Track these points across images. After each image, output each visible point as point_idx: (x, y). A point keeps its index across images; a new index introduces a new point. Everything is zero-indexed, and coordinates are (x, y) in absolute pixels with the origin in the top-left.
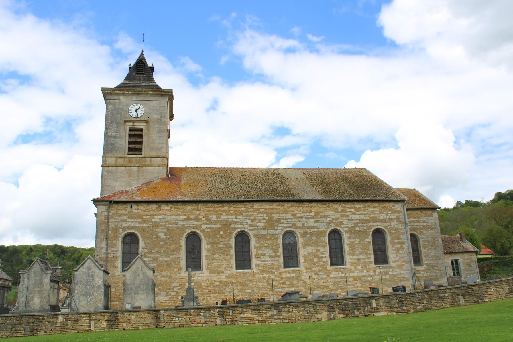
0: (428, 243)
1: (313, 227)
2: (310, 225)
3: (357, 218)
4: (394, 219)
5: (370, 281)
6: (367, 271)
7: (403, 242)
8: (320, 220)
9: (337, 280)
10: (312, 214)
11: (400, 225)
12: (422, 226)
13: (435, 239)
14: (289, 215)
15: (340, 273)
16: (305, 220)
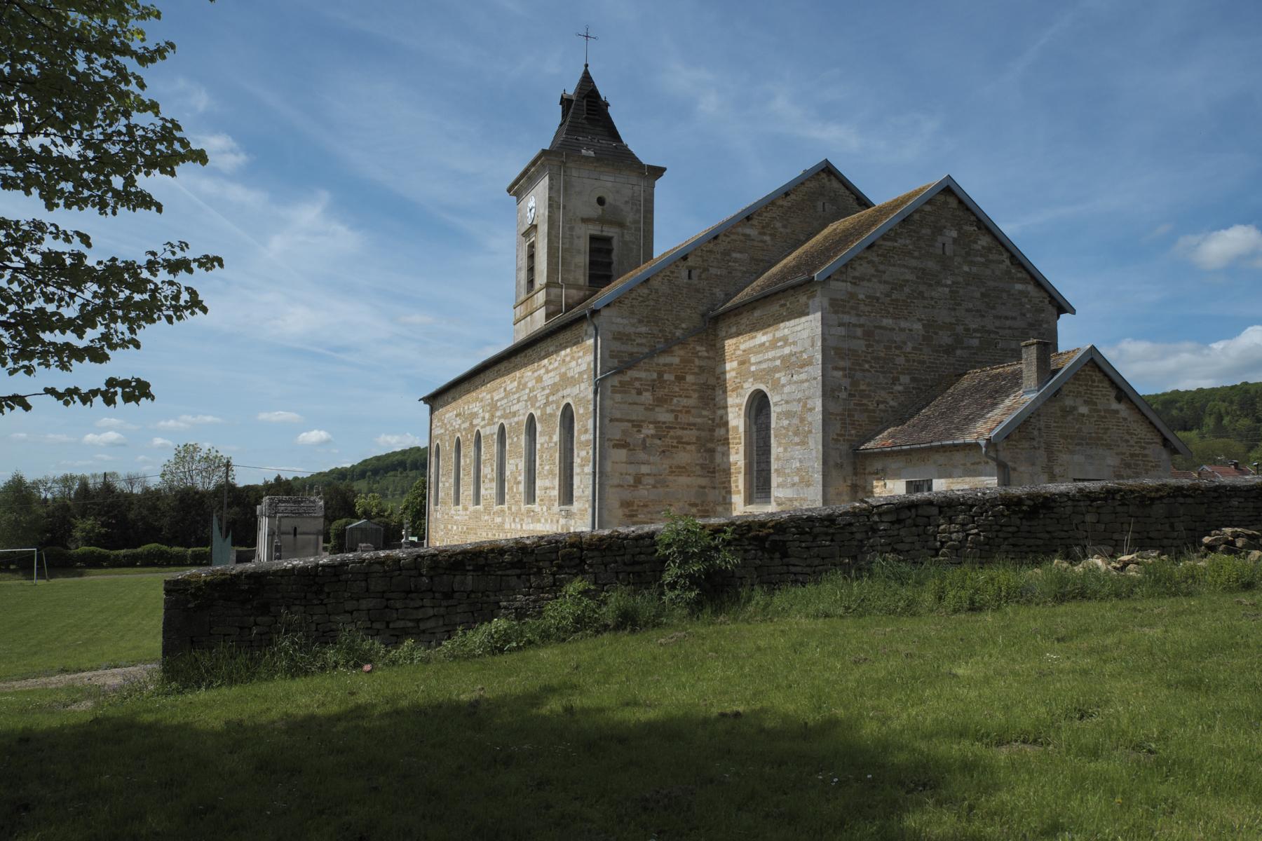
0: (788, 422)
12: (779, 358)
13: (805, 405)
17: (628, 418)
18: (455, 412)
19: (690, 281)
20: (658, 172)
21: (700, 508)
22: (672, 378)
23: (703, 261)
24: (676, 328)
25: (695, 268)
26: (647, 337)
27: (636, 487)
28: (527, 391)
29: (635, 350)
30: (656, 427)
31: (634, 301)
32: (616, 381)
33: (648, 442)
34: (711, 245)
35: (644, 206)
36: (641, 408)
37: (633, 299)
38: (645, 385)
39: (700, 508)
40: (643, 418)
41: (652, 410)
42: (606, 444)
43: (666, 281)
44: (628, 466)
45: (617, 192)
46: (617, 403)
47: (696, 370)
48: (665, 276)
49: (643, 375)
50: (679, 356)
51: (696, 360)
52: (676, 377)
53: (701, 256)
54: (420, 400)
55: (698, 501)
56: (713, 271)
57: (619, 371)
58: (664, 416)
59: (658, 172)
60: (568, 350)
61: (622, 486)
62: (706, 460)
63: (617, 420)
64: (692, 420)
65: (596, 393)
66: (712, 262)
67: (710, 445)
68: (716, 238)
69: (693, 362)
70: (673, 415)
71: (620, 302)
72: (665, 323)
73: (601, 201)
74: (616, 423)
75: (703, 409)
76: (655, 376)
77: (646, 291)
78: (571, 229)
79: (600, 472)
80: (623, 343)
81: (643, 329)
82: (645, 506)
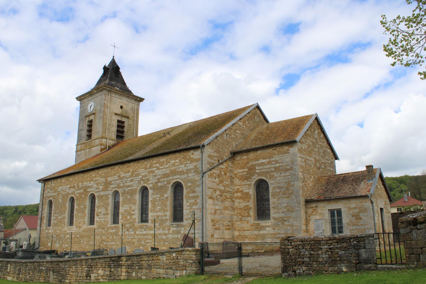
0: (279, 190)
1: (129, 186)
2: (128, 184)
3: (161, 173)
4: (192, 169)
5: (164, 240)
6: (163, 229)
7: (197, 196)
8: (134, 178)
9: (141, 237)
10: (130, 174)
11: (197, 176)
12: (274, 167)
13: (289, 184)
14: (116, 177)
15: (143, 230)
16: (125, 180)
18: (69, 186)
20: (141, 100)
27: (215, 214)
28: (140, 177)
30: (220, 192)
35: (136, 112)
39: (231, 223)
41: (219, 185)
44: (213, 206)
45: (127, 105)
47: (229, 171)
50: (225, 166)
51: (229, 167)
54: (37, 181)
58: (222, 188)
59: (141, 100)
61: (211, 214)
69: (228, 169)
73: (121, 107)
76: (219, 172)
78: (111, 116)
80: (211, 159)
81: (216, 154)
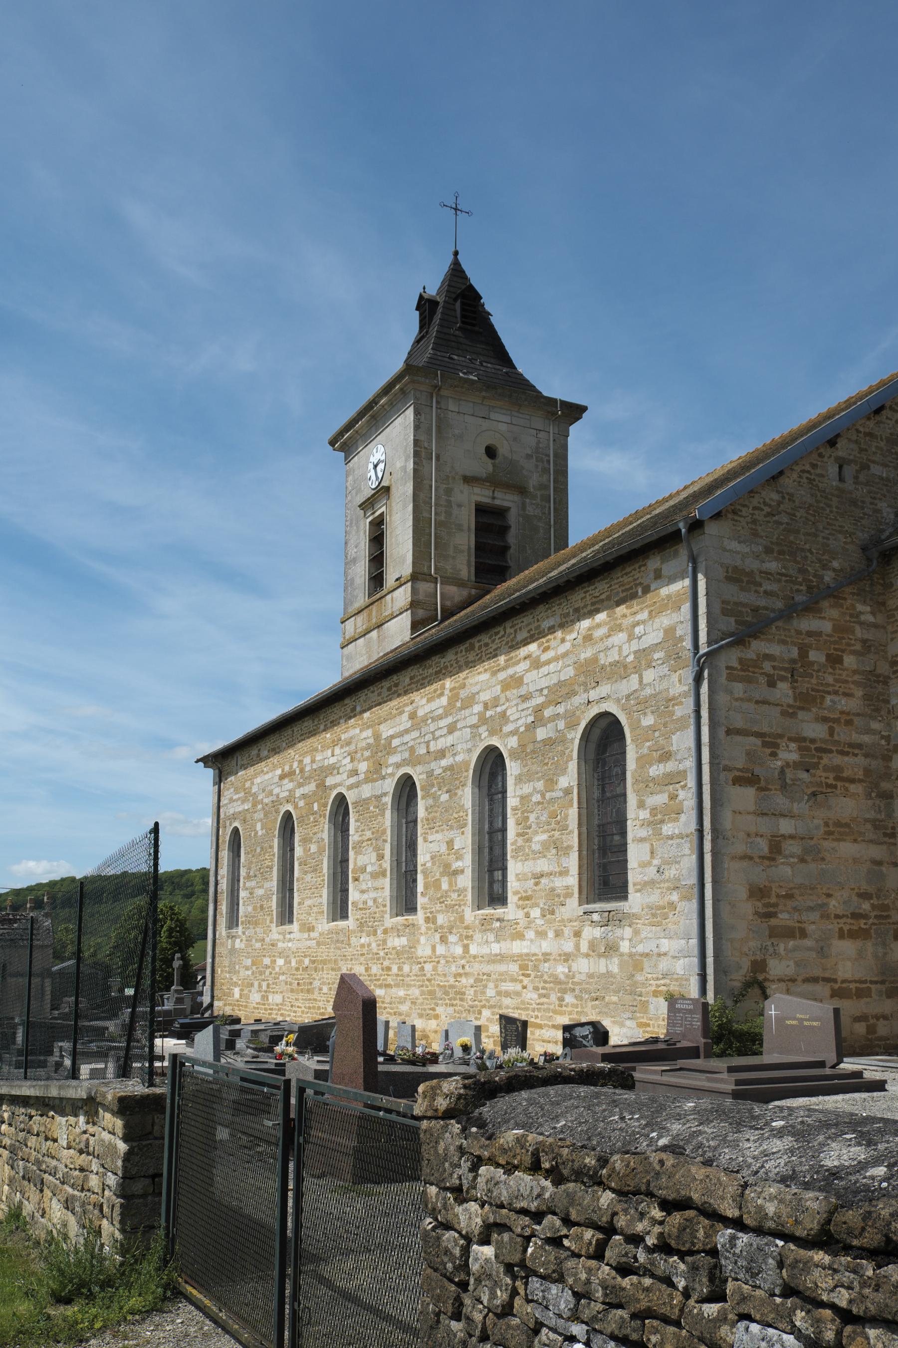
1: (442, 754)
2: (441, 743)
3: (544, 683)
4: (655, 647)
5: (560, 983)
6: (558, 934)
7: (679, 773)
8: (459, 717)
9: (487, 968)
10: (444, 701)
11: (675, 677)
14: (404, 722)
15: (491, 937)
16: (432, 727)
17: (755, 729)
18: (279, 772)
19: (841, 485)
20: (574, 412)
21: (874, 901)
22: (822, 659)
23: (861, 450)
24: (825, 567)
25: (849, 462)
26: (779, 581)
27: (774, 859)
28: (478, 708)
29: (762, 602)
30: (800, 749)
31: (756, 512)
32: (732, 657)
33: (789, 774)
34: (871, 424)
35: (555, 464)
36: (775, 712)
37: (755, 508)
38: (782, 669)
39: (874, 901)
40: (779, 731)
41: (793, 715)
42: (723, 776)
43: (805, 481)
44: (759, 819)
45: (515, 439)
46: (737, 700)
47: (858, 647)
48: (803, 471)
49: (775, 649)
50: (830, 619)
51: (858, 629)
52: (828, 656)
53: (856, 442)
54: (197, 761)
55: (871, 889)
56: (876, 470)
57: (740, 641)
58: (815, 730)
59: (574, 412)
60: (601, 617)
61: (751, 858)
62: (880, 812)
63: (739, 732)
64: (856, 738)
65: (698, 680)
66: (875, 453)
67: (885, 786)
68: (878, 411)
69: (853, 633)
70: (826, 727)
71: (734, 512)
72: (806, 558)
73: (491, 452)
74: (739, 738)
75: (874, 718)
76: (795, 653)
77: (775, 496)
78: (449, 492)
79: (715, 830)
80: (742, 589)
81: (773, 566)
82: (789, 896)
